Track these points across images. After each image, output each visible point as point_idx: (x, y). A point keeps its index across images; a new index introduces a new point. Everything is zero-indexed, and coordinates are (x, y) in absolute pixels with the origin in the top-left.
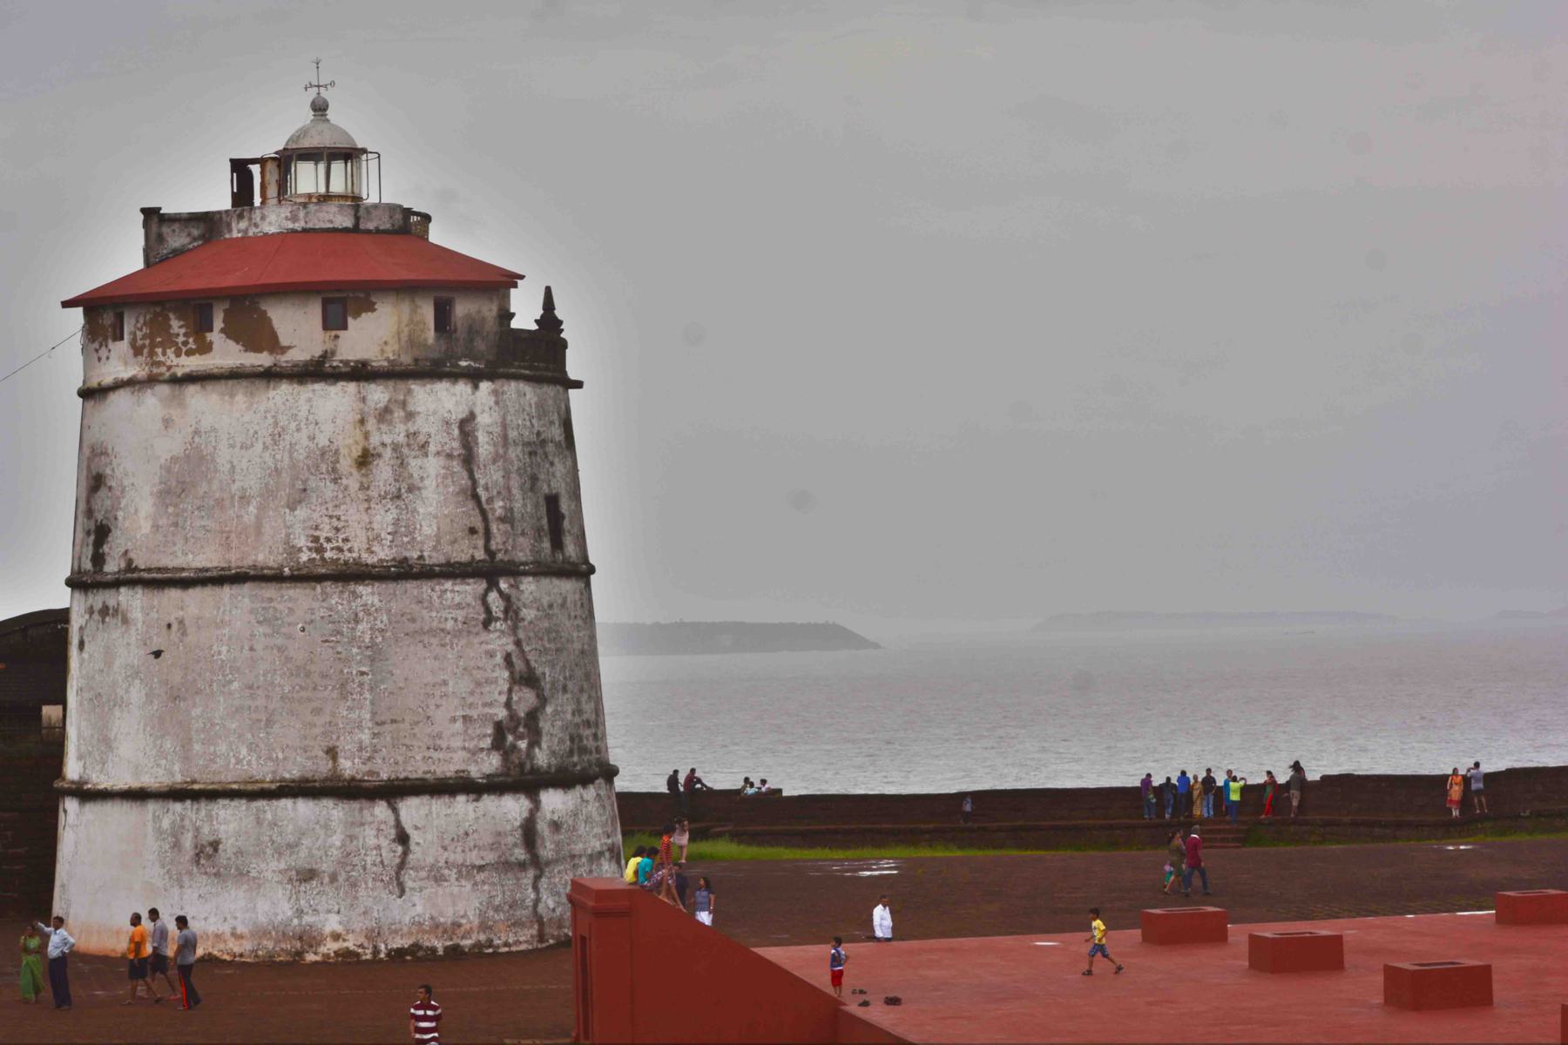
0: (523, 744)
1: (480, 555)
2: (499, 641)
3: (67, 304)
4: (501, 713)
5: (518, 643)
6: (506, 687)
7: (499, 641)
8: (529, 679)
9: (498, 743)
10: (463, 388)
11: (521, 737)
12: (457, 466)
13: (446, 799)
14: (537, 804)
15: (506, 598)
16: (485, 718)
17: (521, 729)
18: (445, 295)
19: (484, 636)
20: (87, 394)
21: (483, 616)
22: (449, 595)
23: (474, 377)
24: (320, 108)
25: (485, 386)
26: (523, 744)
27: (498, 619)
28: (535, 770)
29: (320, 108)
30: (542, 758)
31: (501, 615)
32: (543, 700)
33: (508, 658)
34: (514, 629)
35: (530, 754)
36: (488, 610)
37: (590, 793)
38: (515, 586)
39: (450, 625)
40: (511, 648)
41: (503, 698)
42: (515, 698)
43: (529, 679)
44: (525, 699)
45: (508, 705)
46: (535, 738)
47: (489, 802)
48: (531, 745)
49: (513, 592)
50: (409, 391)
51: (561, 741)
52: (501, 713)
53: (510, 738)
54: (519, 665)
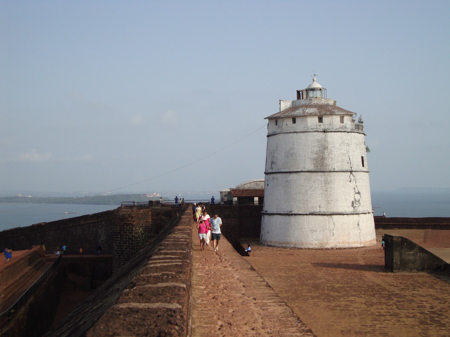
2: (352, 184)
3: (265, 118)
8: (359, 193)
9: (352, 206)
20: (268, 136)
43: (359, 193)
44: (357, 197)
47: (351, 216)
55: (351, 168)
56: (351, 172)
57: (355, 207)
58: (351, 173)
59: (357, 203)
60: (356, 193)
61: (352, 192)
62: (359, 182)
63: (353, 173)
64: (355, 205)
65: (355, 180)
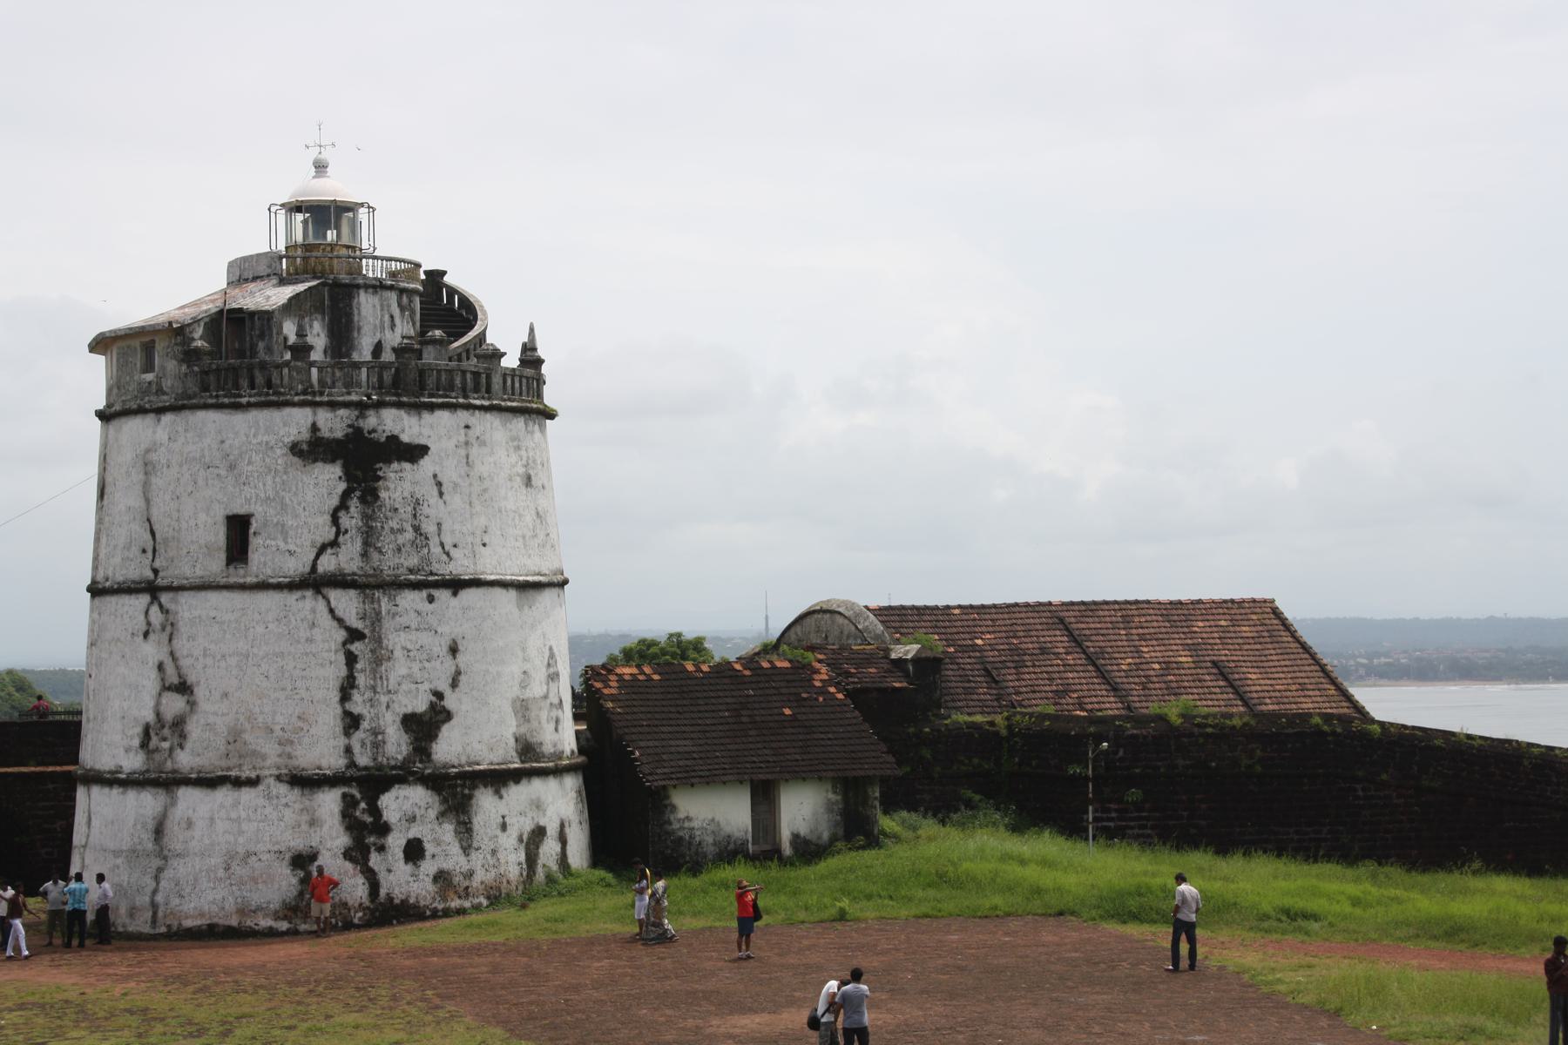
2: (152, 651)
4: (150, 716)
5: (172, 654)
6: (154, 692)
7: (152, 651)
8: (183, 688)
9: (144, 744)
10: (150, 419)
13: (106, 790)
14: (174, 803)
18: (147, 339)
21: (144, 628)
24: (320, 167)
29: (320, 167)
30: (185, 760)
32: (192, 704)
33: (160, 667)
36: (149, 624)
37: (247, 794)
38: (175, 601)
41: (152, 704)
43: (183, 688)
44: (174, 704)
47: (132, 795)
48: (171, 750)
54: (170, 669)
55: (156, 572)
56: (152, 589)
57: (157, 750)
58: (154, 598)
59: (166, 732)
60: (167, 688)
61: (151, 682)
62: (191, 638)
63: (165, 598)
64: (154, 741)
65: (170, 628)
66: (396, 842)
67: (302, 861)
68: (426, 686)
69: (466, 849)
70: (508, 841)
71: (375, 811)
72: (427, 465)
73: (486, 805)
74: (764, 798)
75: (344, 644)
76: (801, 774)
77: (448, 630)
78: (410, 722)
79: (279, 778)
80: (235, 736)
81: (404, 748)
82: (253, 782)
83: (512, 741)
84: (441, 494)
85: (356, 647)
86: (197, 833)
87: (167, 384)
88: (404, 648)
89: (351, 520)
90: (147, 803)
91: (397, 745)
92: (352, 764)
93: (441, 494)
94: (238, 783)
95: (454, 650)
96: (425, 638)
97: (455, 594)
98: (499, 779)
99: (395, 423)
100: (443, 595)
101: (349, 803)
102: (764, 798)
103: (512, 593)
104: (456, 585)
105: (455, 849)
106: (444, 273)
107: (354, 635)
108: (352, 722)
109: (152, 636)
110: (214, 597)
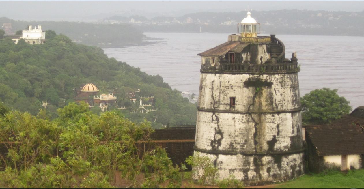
0: (216, 145)
1: (213, 108)
4: (213, 139)
5: (218, 126)
7: (214, 125)
9: (212, 144)
10: (213, 75)
11: (216, 144)
12: (211, 90)
14: (218, 157)
15: (216, 117)
16: (210, 140)
17: (216, 142)
19: (212, 123)
21: (212, 120)
22: (207, 115)
23: (216, 73)
25: (218, 75)
26: (216, 145)
27: (214, 121)
28: (218, 150)
30: (221, 148)
31: (215, 120)
32: (222, 137)
33: (215, 128)
34: (218, 123)
35: (218, 147)
37: (234, 157)
39: (207, 121)
40: (216, 126)
41: (214, 136)
42: (216, 136)
45: (214, 137)
46: (220, 144)
49: (218, 116)
50: (206, 75)
51: (226, 146)
52: (213, 139)
53: (214, 144)
56: (214, 111)
58: (214, 114)
61: (213, 132)
66: (265, 168)
67: (245, 171)
68: (272, 135)
69: (280, 170)
70: (288, 168)
71: (261, 162)
72: (273, 86)
73: (285, 161)
74: (344, 157)
75: (255, 126)
76: (352, 153)
77: (277, 122)
78: (269, 143)
79: (241, 154)
80: (231, 144)
81: (267, 148)
82: (236, 154)
83: (289, 146)
84: (276, 93)
85: (257, 126)
86: (223, 164)
87: (217, 67)
88: (267, 127)
89: (257, 100)
90: (212, 157)
91: (265, 147)
92: (256, 151)
93: (276, 93)
94: (232, 154)
95: (278, 126)
96: (272, 124)
97: (278, 115)
98: (287, 154)
99: (265, 77)
100: (276, 115)
101: (255, 160)
102: (344, 157)
103: (290, 114)
104: (279, 113)
105: (278, 169)
106: (274, 35)
107: (256, 124)
108: (256, 143)
109: (213, 122)
110: (227, 114)
